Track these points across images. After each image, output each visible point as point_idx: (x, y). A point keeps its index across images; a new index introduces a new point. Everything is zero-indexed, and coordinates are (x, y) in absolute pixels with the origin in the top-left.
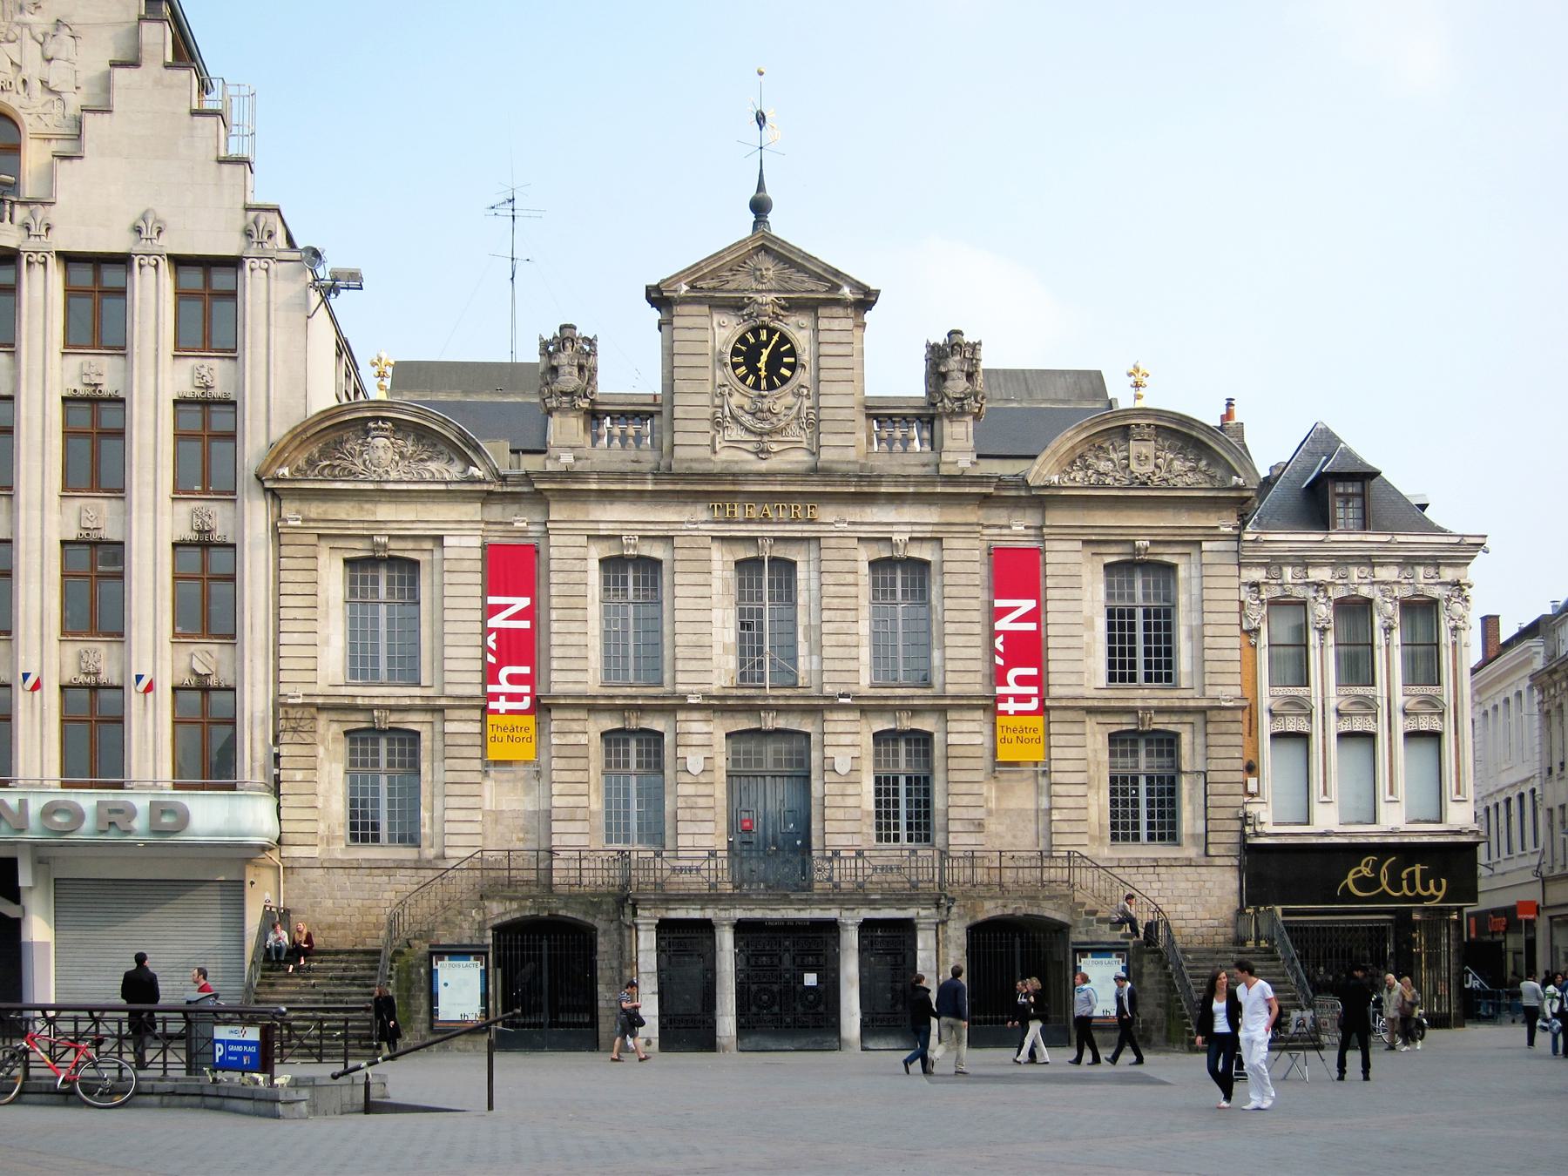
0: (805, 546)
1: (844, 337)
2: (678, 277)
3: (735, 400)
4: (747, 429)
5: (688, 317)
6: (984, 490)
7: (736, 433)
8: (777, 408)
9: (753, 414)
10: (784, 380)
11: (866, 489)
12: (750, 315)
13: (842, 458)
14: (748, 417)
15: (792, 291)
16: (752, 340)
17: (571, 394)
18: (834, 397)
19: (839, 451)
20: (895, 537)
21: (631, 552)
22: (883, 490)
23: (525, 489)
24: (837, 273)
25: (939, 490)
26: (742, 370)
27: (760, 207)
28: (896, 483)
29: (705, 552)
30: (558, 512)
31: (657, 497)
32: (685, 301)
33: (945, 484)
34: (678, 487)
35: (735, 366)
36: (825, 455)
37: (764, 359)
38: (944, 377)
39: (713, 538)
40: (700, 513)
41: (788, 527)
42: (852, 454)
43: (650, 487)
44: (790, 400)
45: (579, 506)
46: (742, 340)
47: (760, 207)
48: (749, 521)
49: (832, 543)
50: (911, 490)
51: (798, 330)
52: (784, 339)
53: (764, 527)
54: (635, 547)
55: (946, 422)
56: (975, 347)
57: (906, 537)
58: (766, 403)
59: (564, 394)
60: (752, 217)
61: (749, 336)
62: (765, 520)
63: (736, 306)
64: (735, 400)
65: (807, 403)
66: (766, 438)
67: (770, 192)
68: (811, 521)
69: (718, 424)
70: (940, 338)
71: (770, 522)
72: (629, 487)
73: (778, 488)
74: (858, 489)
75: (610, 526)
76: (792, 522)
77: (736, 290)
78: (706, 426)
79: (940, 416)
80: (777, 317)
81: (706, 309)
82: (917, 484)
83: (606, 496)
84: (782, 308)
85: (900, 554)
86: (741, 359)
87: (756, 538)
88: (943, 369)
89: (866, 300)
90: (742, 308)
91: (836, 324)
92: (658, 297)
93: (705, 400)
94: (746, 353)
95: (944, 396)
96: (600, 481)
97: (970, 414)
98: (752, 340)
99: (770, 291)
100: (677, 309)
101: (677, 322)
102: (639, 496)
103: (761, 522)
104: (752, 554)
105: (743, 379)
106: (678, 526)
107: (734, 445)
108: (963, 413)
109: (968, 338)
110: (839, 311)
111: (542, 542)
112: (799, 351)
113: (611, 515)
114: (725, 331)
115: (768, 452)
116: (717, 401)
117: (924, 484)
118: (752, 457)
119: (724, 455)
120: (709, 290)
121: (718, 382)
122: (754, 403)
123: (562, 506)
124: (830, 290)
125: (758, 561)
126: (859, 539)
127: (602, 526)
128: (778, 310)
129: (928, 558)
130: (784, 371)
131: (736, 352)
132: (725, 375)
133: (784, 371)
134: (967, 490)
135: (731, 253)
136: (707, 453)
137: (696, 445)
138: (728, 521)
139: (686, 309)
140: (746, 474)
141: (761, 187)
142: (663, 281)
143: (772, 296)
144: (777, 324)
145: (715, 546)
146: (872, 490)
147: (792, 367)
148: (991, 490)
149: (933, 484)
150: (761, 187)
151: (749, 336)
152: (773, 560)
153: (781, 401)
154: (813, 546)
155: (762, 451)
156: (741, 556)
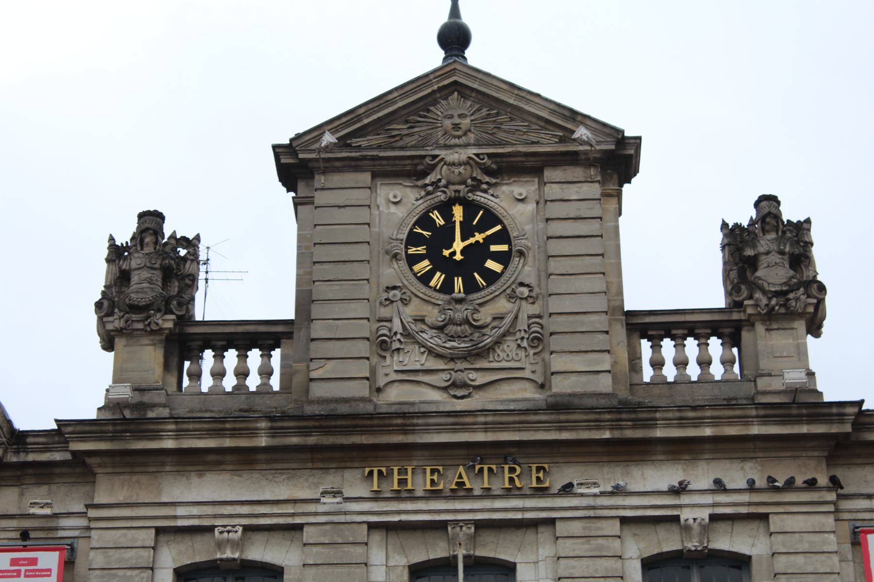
0: (530, 536)
1: (585, 209)
2: (319, 129)
3: (413, 309)
4: (431, 352)
5: (342, 190)
6: (835, 429)
7: (414, 359)
8: (485, 316)
9: (441, 329)
10: (492, 277)
11: (630, 434)
12: (435, 184)
13: (590, 389)
14: (433, 332)
15: (501, 144)
16: (440, 222)
17: (145, 308)
18: (574, 297)
19: (584, 378)
20: (686, 515)
21: (228, 554)
22: (659, 433)
23: (58, 456)
24: (574, 115)
25: (756, 430)
26: (424, 266)
27: (454, 38)
28: (682, 422)
29: (360, 550)
30: (107, 491)
31: (275, 459)
32: (330, 166)
33: (765, 420)
34: (312, 440)
35: (413, 260)
36: (561, 386)
37: (458, 252)
38: (753, 263)
39: (372, 526)
40: (354, 484)
41: (499, 504)
42: (605, 384)
43: (263, 441)
44: (503, 305)
45: (144, 479)
46: (425, 221)
47: (454, 38)
48: (434, 494)
49: (576, 528)
50: (708, 432)
51: (514, 203)
52: (491, 218)
53: (458, 505)
54: (236, 545)
55: (760, 328)
56: (802, 228)
57: (704, 514)
58: (461, 312)
59: (134, 308)
60: (441, 54)
61: (436, 216)
62: (461, 492)
63: (414, 171)
64: (413, 309)
65: (528, 309)
66: (460, 365)
67: (467, 18)
68: (541, 492)
69: (383, 346)
70: (744, 214)
71: (469, 495)
72: (228, 443)
73: (480, 437)
74: (617, 434)
75: (195, 511)
76: (509, 493)
77: (414, 147)
78: (363, 349)
79: (750, 323)
80: (477, 186)
81: (365, 178)
82: (716, 421)
83: (191, 461)
84: (488, 172)
85: (692, 545)
86: (421, 250)
87: (440, 527)
88: (749, 252)
89: (618, 158)
90: (424, 174)
91: (573, 192)
92: (297, 165)
93: (361, 309)
94: (428, 237)
95: (755, 286)
96: (179, 434)
97: (800, 315)
98: (440, 222)
99: (466, 145)
100: (320, 180)
101: (321, 198)
102: (245, 460)
103: (453, 495)
104: (438, 550)
105: (425, 279)
106: (312, 508)
107: (409, 376)
108: (791, 315)
109: (789, 213)
110: (578, 173)
111: (81, 545)
112: (513, 234)
113: (195, 494)
114: (397, 206)
115: (465, 385)
116: (384, 312)
117: (730, 421)
118: (435, 396)
119: (395, 395)
120: (370, 148)
121: (386, 282)
122: (442, 311)
123: (117, 480)
124: (562, 140)
125: (447, 565)
126: (624, 521)
127: (180, 511)
128: (478, 174)
129: (745, 550)
130: (491, 264)
131: (413, 239)
132: (393, 272)
133: (491, 264)
134: (804, 429)
135: (403, 96)
136: (361, 390)
137: (340, 379)
138: (397, 496)
139: (336, 179)
140: (425, 414)
141: (455, 11)
142: (299, 136)
143: (472, 151)
144: (479, 197)
145: (377, 537)
146: (638, 434)
147: (503, 258)
148: (848, 428)
149: (745, 420)
150: (455, 11)
151: (436, 216)
152: (475, 564)
153: (495, 307)
154: (544, 533)
155: (454, 385)
156: (419, 556)
